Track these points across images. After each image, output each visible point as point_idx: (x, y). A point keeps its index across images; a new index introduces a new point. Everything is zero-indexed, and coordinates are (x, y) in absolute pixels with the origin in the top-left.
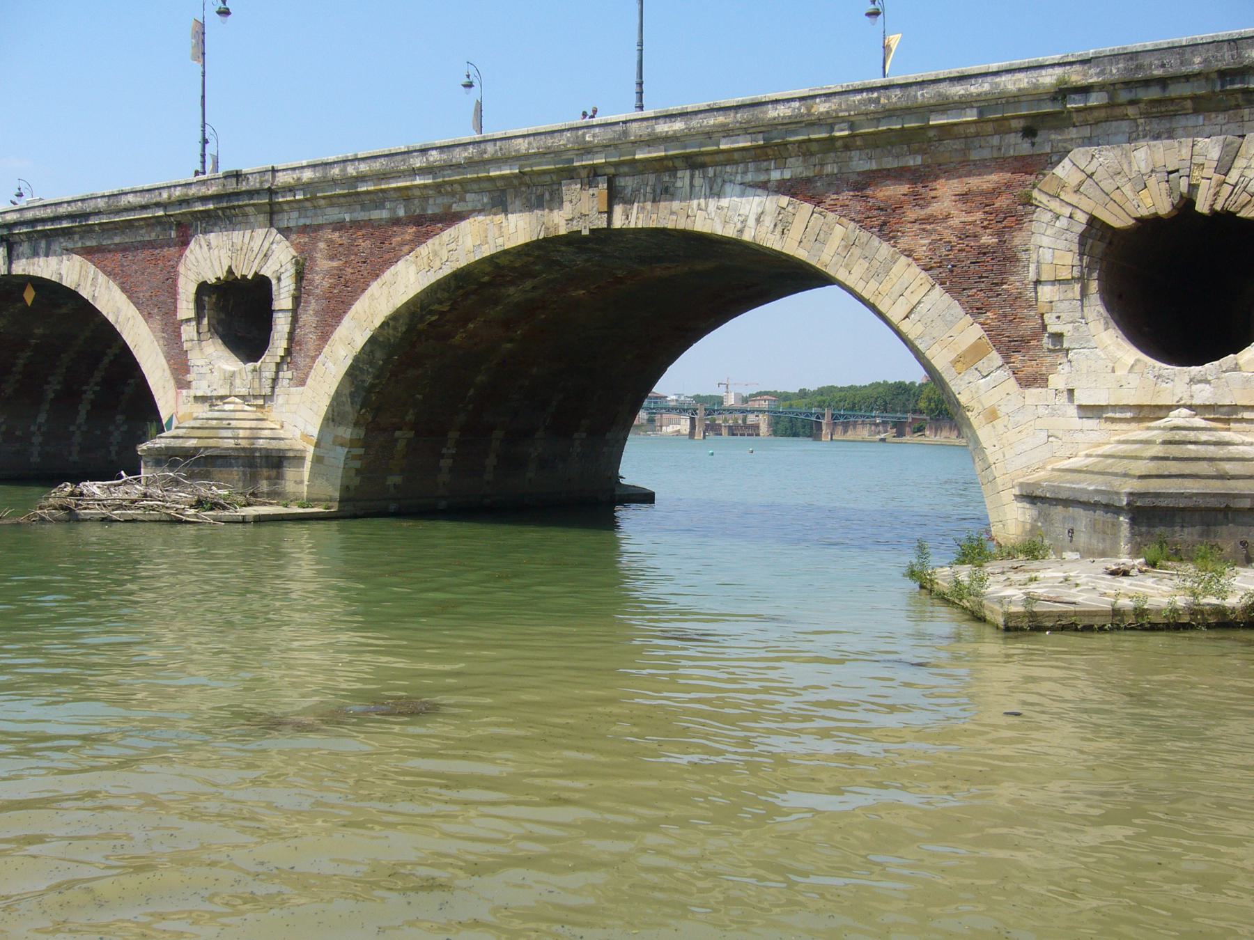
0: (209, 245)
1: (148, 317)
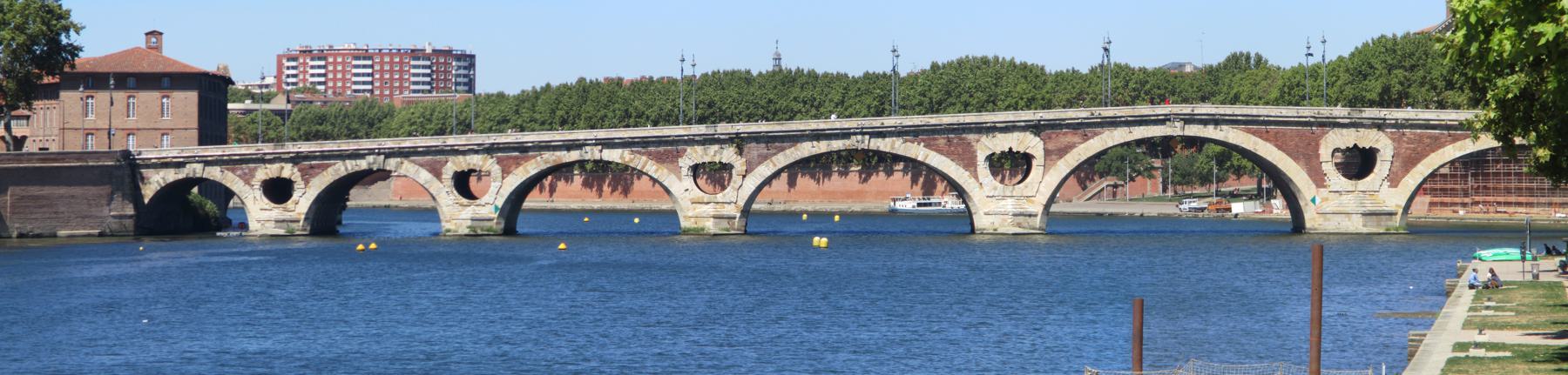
0: (1342, 135)
1: (1296, 159)
